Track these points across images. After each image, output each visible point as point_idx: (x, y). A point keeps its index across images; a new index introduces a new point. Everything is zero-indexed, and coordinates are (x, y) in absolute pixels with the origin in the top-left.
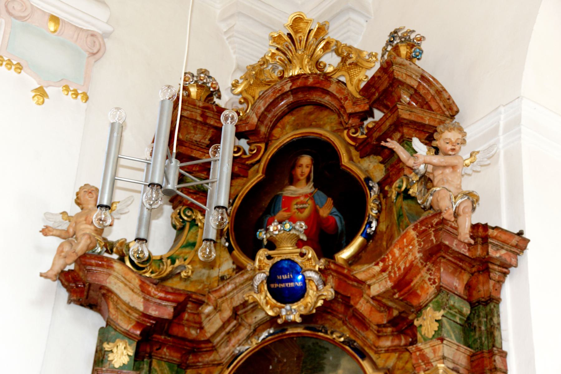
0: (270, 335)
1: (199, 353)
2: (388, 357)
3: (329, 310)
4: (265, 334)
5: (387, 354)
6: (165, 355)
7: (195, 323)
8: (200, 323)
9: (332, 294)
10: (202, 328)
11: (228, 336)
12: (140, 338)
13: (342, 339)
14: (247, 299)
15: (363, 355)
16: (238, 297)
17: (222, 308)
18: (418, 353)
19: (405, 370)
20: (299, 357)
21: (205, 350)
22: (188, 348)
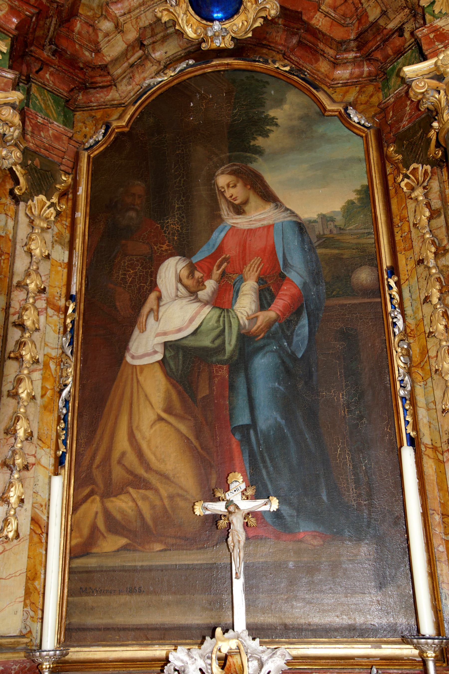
0: (189, 66)
1: (92, 91)
2: (347, 92)
3: (264, 42)
4: (184, 65)
5: (344, 88)
6: (49, 82)
7: (90, 41)
8: (97, 43)
9: (277, 7)
10: (98, 51)
11: (131, 69)
12: (16, 33)
13: (287, 69)
14: (159, 15)
15: (317, 88)
16: (146, 16)
17: (125, 29)
18: (432, 36)
19: (370, 104)
20: (229, 93)
21: (101, 85)
22: (78, 79)
